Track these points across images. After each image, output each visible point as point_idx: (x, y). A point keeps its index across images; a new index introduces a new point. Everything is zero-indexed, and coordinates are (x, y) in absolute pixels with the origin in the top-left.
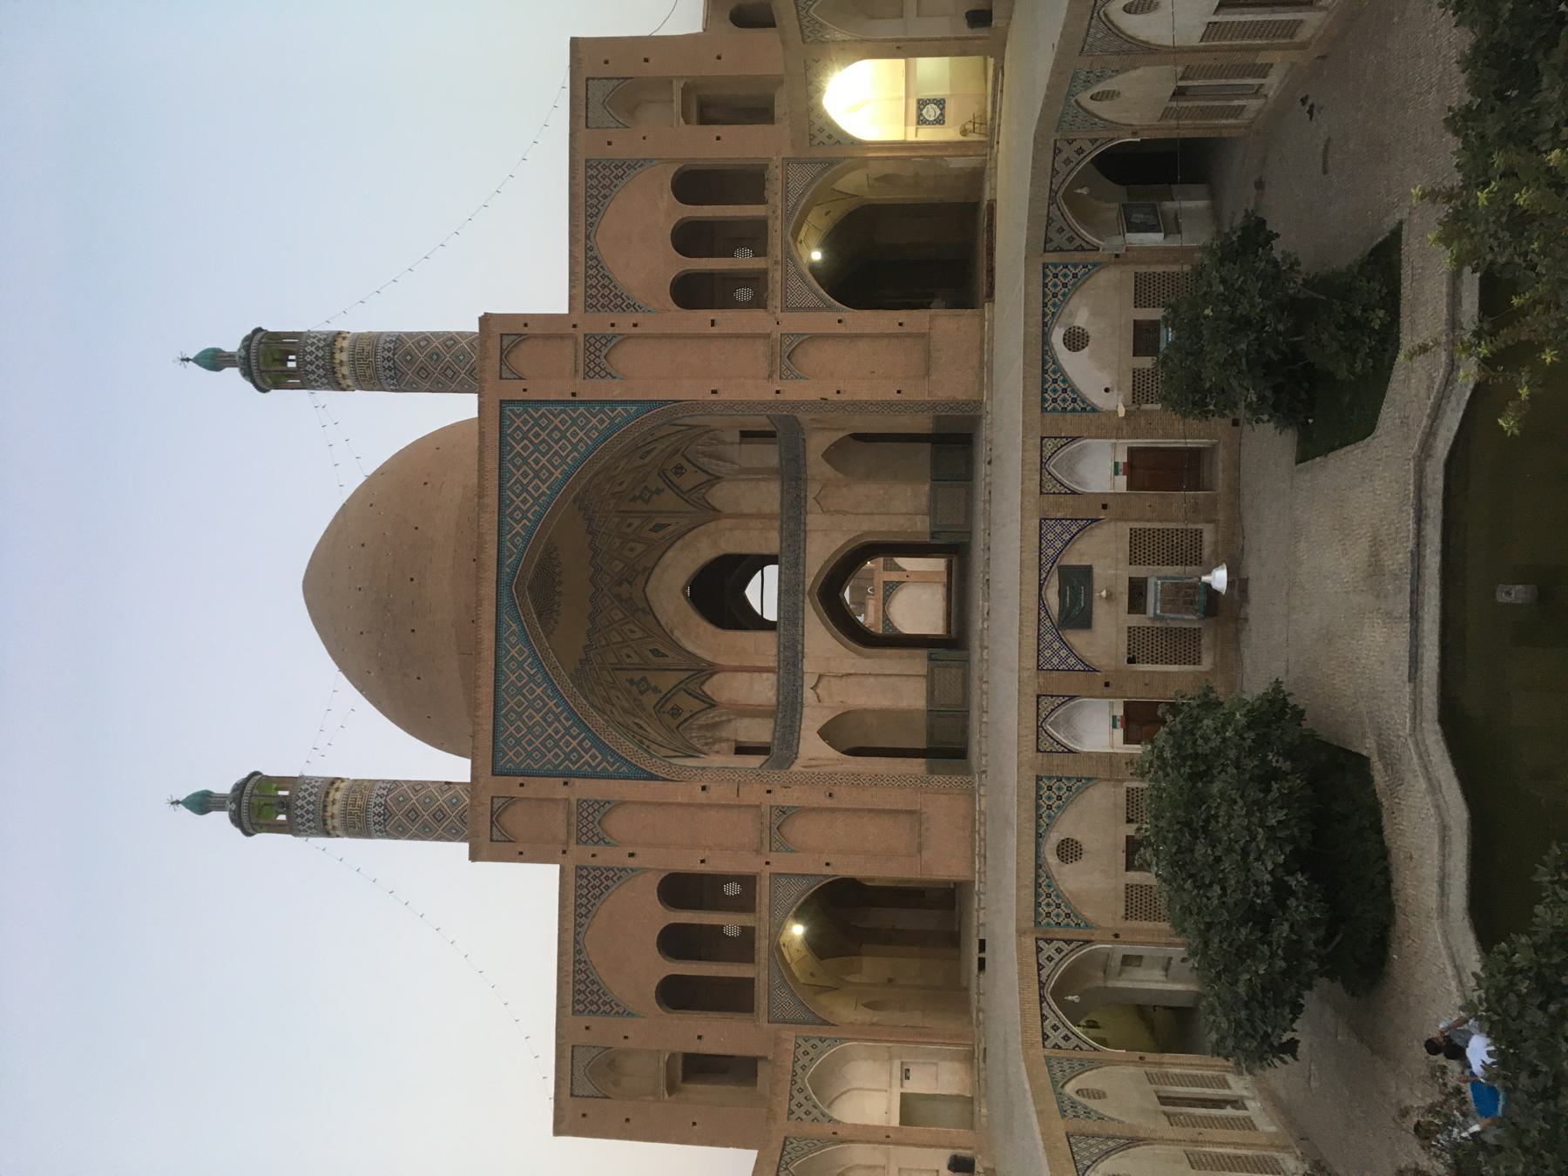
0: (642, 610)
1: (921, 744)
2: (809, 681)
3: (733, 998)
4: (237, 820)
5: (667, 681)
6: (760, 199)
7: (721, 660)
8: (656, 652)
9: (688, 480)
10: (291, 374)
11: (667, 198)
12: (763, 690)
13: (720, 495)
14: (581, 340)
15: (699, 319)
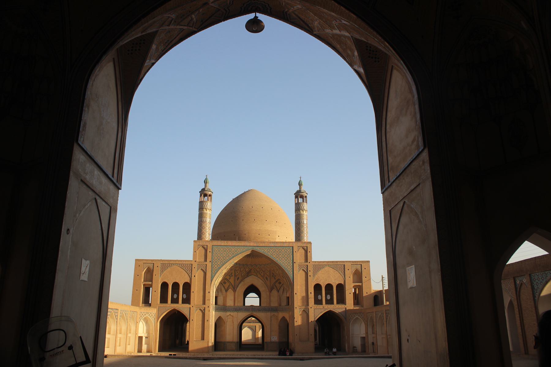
0: (248, 274)
1: (217, 340)
2: (232, 314)
3: (164, 299)
4: (203, 190)
5: (232, 280)
6: (338, 303)
7: (236, 293)
8: (238, 279)
9: (277, 284)
10: (298, 200)
11: (338, 283)
12: (230, 303)
13: (274, 292)
14: (307, 264)
15: (311, 290)
